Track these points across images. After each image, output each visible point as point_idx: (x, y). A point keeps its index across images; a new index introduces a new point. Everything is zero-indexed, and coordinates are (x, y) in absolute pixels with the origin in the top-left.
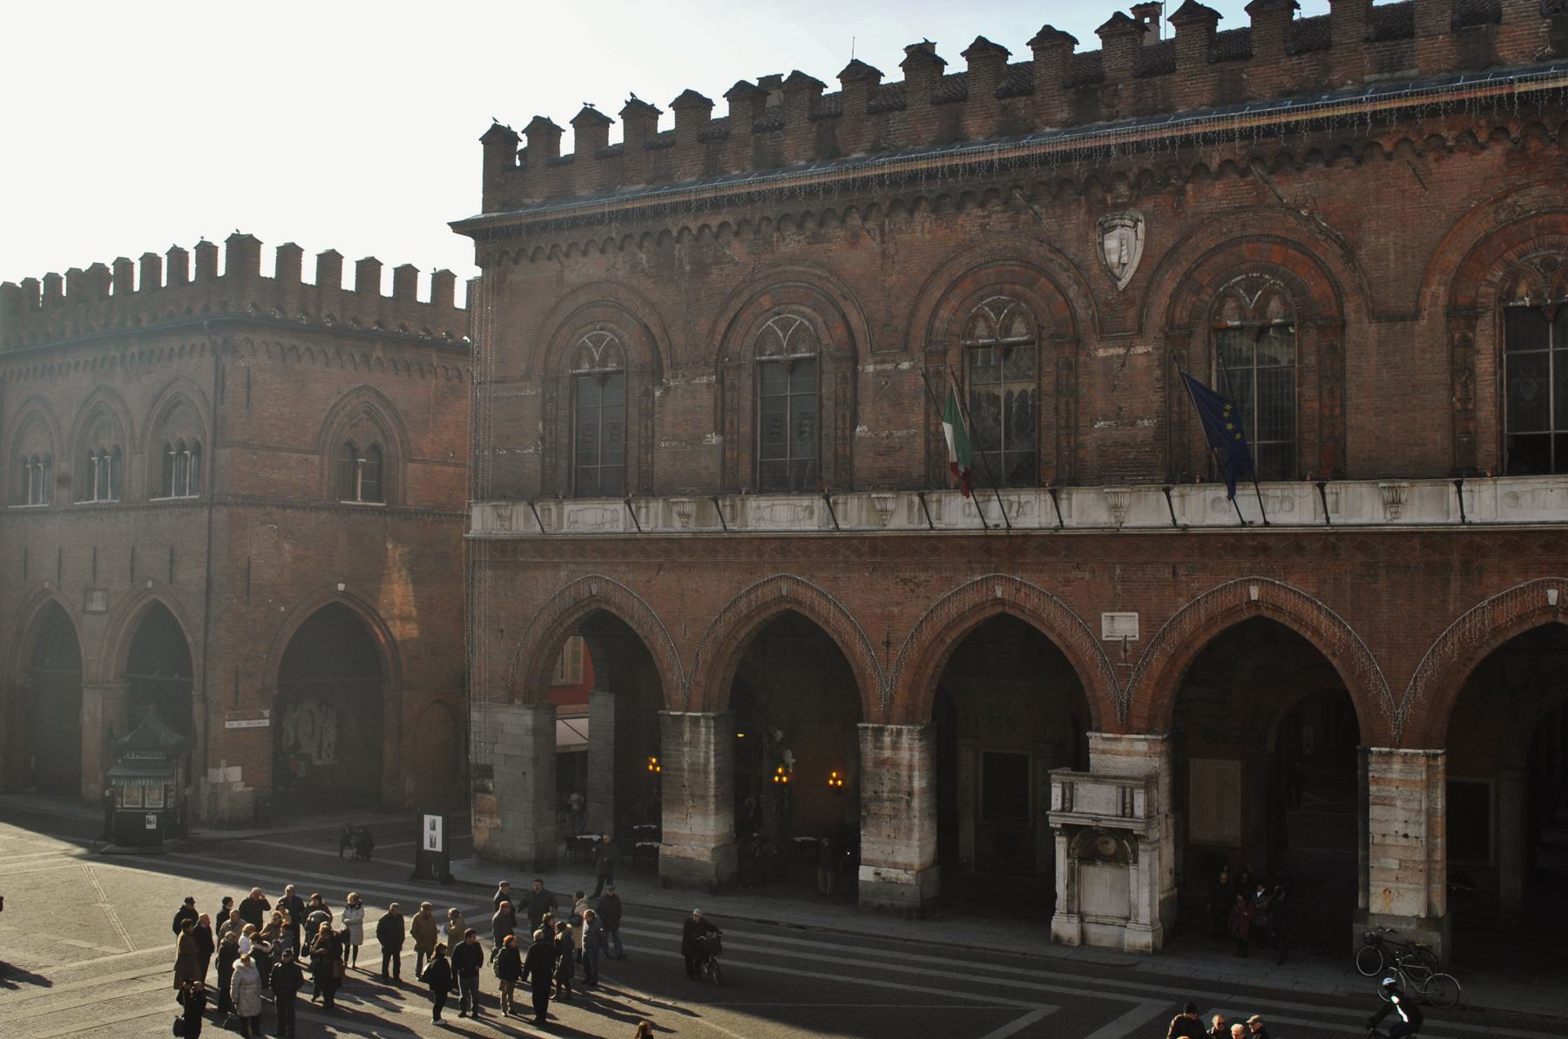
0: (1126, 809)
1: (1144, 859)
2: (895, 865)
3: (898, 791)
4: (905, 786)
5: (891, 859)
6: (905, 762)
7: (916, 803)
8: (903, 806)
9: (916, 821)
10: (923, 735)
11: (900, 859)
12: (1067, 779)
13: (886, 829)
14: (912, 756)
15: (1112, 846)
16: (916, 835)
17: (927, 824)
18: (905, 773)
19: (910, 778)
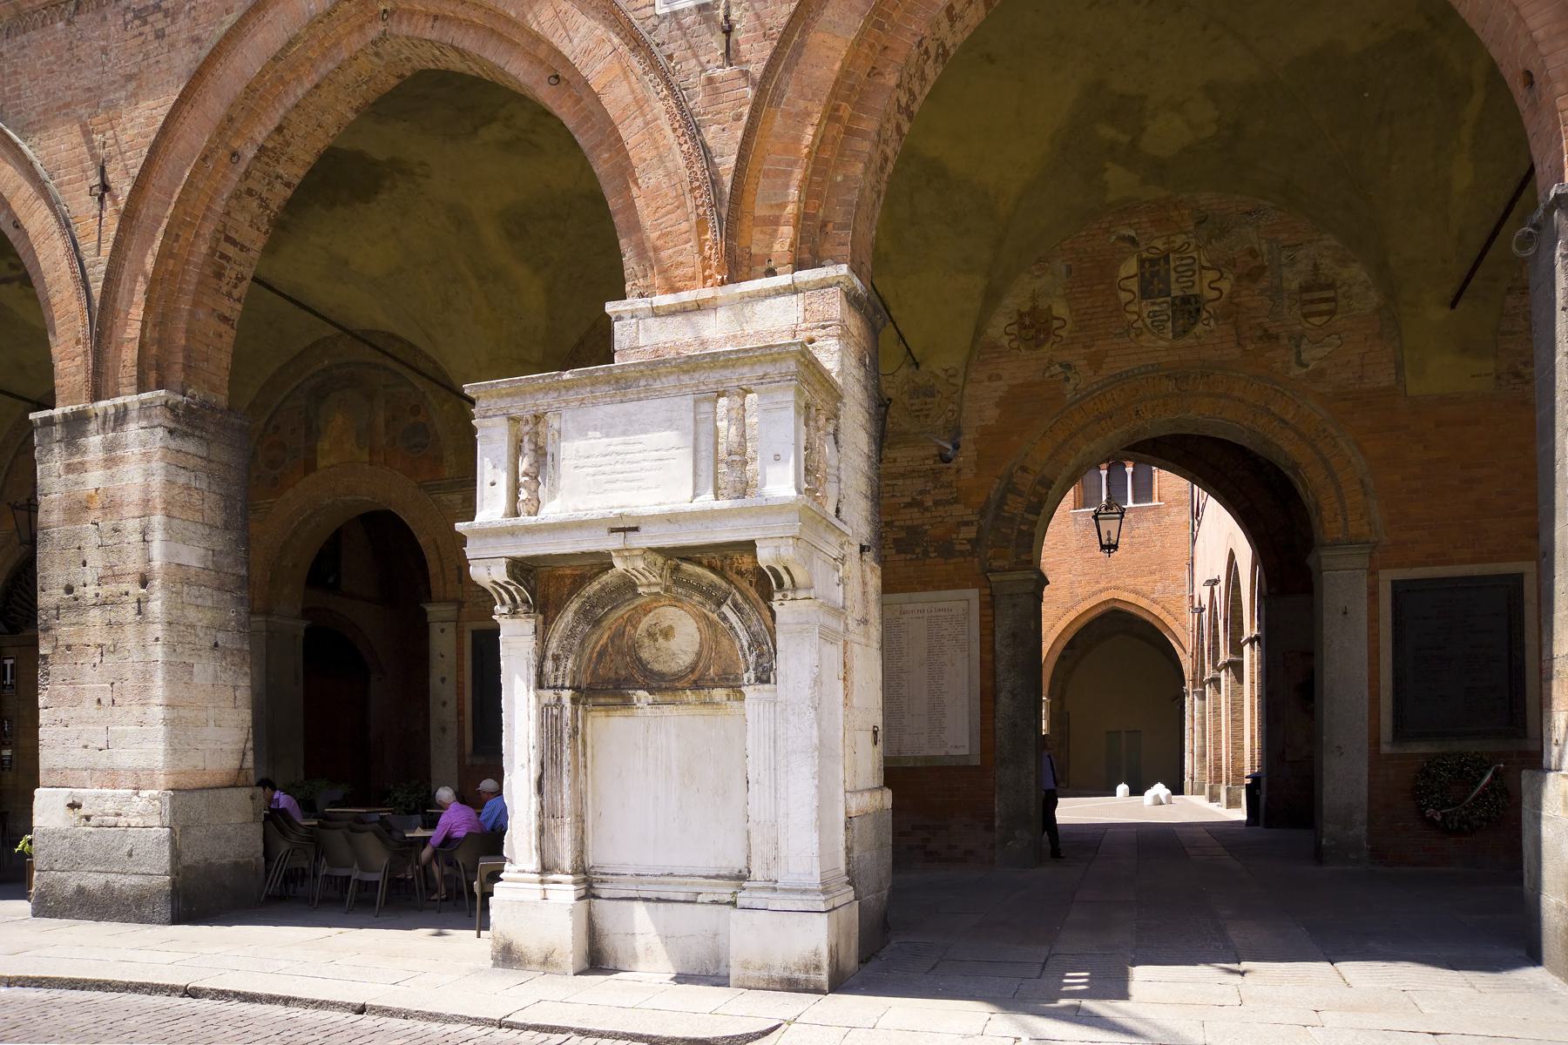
0: (729, 468)
1: (801, 656)
2: (111, 777)
3: (116, 577)
4: (134, 564)
5: (103, 760)
6: (135, 495)
7: (156, 607)
8: (129, 613)
9: (158, 652)
10: (185, 421)
11: (125, 758)
12: (518, 408)
13: (93, 681)
14: (148, 474)
15: (681, 636)
16: (158, 691)
17: (205, 670)
18: (132, 525)
19: (144, 533)
